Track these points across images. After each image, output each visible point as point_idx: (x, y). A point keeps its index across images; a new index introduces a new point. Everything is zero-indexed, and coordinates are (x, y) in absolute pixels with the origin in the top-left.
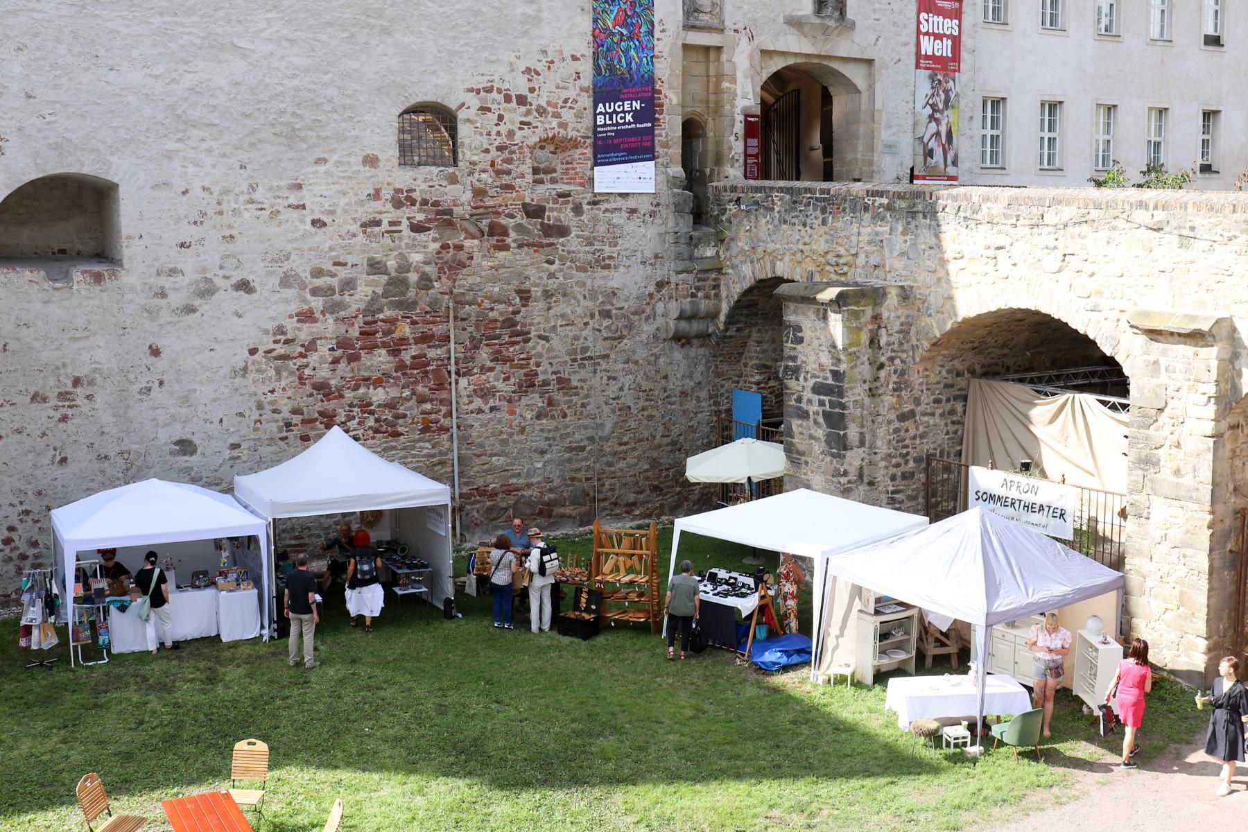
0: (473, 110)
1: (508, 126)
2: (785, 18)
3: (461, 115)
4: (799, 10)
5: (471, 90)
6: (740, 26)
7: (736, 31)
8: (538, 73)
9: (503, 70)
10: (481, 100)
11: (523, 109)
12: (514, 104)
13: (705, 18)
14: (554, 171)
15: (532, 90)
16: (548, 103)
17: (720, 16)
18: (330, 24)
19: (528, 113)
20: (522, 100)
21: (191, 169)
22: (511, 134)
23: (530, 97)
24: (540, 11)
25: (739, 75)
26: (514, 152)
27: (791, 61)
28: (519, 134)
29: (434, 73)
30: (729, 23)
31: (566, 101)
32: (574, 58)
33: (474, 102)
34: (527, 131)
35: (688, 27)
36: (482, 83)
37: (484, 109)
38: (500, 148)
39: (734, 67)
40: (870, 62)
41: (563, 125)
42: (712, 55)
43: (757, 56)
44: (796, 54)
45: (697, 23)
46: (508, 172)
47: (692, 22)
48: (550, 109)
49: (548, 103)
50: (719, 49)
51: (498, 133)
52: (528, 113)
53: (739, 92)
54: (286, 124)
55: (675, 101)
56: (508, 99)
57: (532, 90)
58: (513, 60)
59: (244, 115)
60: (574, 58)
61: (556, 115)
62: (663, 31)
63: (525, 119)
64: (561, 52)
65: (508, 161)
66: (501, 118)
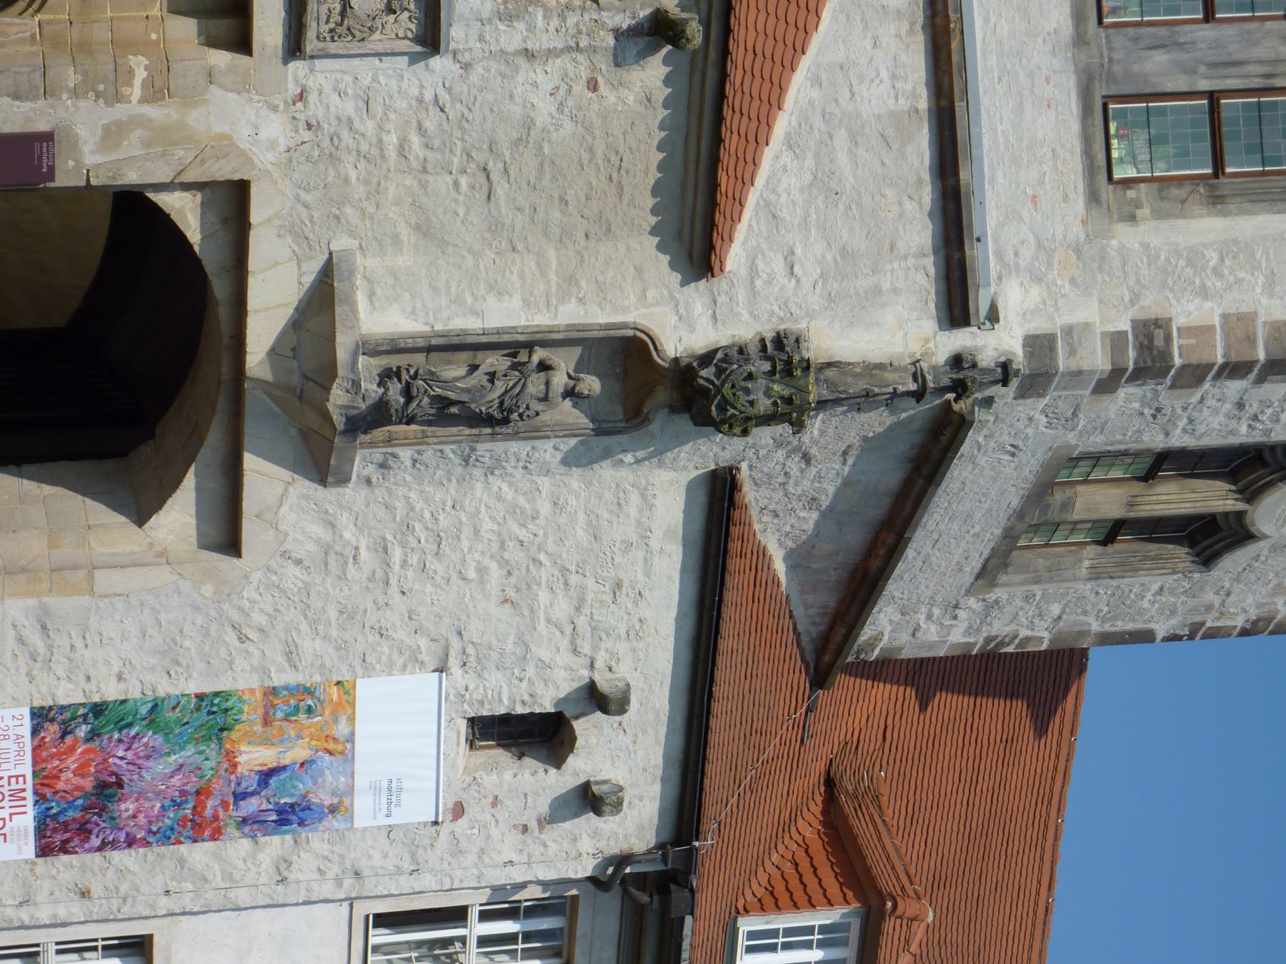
2: (347, 253)
4: (371, 295)
6: (315, 109)
7: (301, 97)
27: (220, 288)
42: (223, 26)
53: (120, 112)
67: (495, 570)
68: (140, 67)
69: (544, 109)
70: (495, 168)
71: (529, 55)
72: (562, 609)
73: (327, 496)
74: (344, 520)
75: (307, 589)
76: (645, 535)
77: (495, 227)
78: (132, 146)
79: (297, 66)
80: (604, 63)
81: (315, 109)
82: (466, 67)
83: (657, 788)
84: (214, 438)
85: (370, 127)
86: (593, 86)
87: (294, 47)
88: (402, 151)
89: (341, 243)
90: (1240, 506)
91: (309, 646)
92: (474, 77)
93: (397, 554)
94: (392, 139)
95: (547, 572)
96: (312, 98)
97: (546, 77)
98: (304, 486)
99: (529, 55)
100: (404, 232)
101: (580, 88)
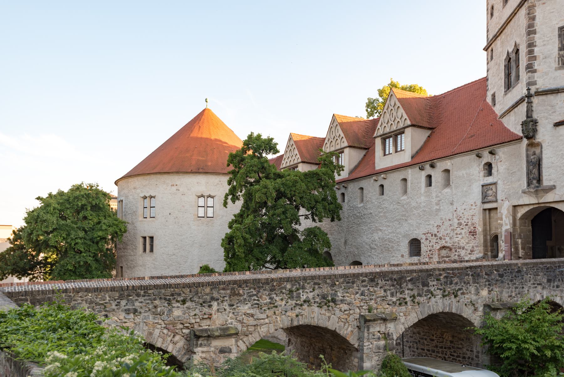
0: (424, 240)
1: (432, 244)
3: (422, 241)
5: (423, 234)
6: (504, 198)
7: (502, 200)
8: (440, 226)
9: (431, 227)
10: (426, 237)
11: (436, 238)
12: (434, 237)
13: (490, 198)
14: (450, 257)
15: (438, 232)
16: (442, 235)
17: (496, 197)
18: (395, 220)
19: (437, 239)
21: (372, 259)
22: (433, 246)
23: (438, 234)
24: (440, 207)
25: (504, 217)
26: (433, 252)
28: (435, 246)
29: (416, 230)
30: (499, 198)
31: (447, 234)
32: (450, 220)
33: (424, 237)
35: (483, 203)
36: (426, 231)
37: (427, 239)
38: (430, 251)
39: (502, 214)
41: (446, 242)
43: (511, 209)
44: (533, 204)
45: (487, 201)
46: (432, 258)
47: (486, 200)
48: (443, 237)
49: (442, 235)
50: (496, 209)
51: (430, 246)
52: (437, 239)
53: (504, 224)
54: (387, 247)
55: (480, 230)
57: (438, 232)
58: (434, 223)
59: (380, 246)
60: (450, 220)
61: (445, 239)
62: (476, 206)
63: (436, 241)
64: (446, 219)
65: (432, 254)
66: (430, 241)
68: (499, 221)
70: (511, 172)
71: (498, 171)
81: (504, 198)
82: (499, 179)
85: (506, 190)
86: (501, 161)
87: (496, 201)
88: (509, 185)
89: (521, 192)
92: (500, 177)
94: (507, 187)
96: (502, 199)
99: (498, 171)
100: (519, 183)
101: (501, 163)
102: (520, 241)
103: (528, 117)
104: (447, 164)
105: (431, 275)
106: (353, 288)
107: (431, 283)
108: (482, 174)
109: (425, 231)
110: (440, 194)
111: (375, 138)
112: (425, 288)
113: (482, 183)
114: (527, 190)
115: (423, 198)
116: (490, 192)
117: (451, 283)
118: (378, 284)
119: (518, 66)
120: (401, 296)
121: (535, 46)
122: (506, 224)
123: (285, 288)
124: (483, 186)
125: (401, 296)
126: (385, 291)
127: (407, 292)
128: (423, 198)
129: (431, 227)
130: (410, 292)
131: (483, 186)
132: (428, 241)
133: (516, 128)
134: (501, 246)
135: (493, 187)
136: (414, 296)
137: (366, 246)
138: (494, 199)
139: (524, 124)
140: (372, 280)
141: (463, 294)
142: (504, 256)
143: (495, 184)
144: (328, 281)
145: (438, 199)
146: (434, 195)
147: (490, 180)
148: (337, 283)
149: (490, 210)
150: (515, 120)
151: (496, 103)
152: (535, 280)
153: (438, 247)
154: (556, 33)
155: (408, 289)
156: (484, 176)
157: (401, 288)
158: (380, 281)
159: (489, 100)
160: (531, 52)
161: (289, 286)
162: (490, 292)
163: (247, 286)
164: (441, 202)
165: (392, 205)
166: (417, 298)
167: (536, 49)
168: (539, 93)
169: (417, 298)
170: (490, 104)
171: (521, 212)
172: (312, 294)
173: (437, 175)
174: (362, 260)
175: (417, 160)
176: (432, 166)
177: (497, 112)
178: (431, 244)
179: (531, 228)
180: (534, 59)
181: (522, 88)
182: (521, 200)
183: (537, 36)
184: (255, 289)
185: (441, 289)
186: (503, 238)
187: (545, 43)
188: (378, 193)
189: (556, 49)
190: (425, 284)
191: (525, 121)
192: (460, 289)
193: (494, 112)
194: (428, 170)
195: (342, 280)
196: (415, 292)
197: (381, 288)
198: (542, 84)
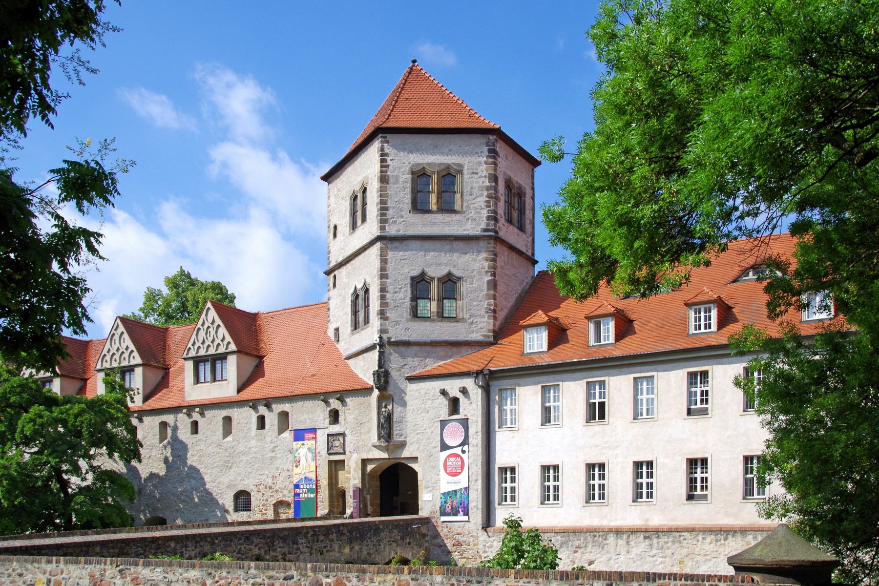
19: (272, 492)
20: (270, 488)
22: (267, 500)
25: (352, 470)
27: (381, 462)
28: (269, 500)
30: (348, 449)
32: (288, 470)
34: (272, 498)
35: (330, 454)
38: (263, 505)
39: (350, 468)
40: (417, 458)
41: (284, 496)
50: (343, 461)
52: (272, 492)
53: (352, 478)
56: (266, 487)
67: (423, 414)
69: (353, 416)
72: (430, 402)
73: (408, 443)
74: (412, 441)
75: (424, 446)
76: (417, 390)
77: (368, 421)
78: (356, 476)
79: (347, 453)
80: (346, 408)
81: (352, 450)
83: (464, 380)
84: (403, 461)
87: (344, 453)
89: (370, 445)
90: (436, 280)
91: (434, 444)
93: (419, 431)
95: (423, 406)
97: (348, 416)
98: (407, 447)
102: (368, 497)
103: (380, 366)
104: (286, 407)
105: (300, 533)
106: (230, 546)
107: (300, 541)
108: (327, 421)
109: (256, 481)
110: (276, 440)
111: (185, 359)
112: (295, 546)
113: (327, 431)
114: (378, 444)
115: (253, 442)
116: (337, 443)
117: (318, 541)
118: (253, 542)
119: (367, 307)
120: (274, 554)
121: (387, 292)
122: (355, 479)
123: (169, 546)
124: (328, 435)
125: (274, 554)
126: (259, 549)
127: (279, 550)
128: (253, 442)
129: (265, 477)
130: (281, 549)
131: (328, 435)
132: (261, 494)
133: (365, 375)
134: (348, 502)
135: (341, 438)
136: (285, 554)
137: (172, 498)
138: (342, 451)
139: (377, 375)
140: (248, 538)
141: (328, 551)
142: (352, 513)
143: (343, 435)
144: (209, 539)
145: (274, 445)
146: (268, 439)
147: (335, 429)
148: (217, 541)
149: (336, 462)
150: (364, 366)
151: (340, 339)
152: (390, 538)
153: (274, 502)
154: (408, 281)
155: (280, 547)
156: (330, 424)
157: (273, 545)
158: (255, 539)
159: (331, 333)
160: (383, 297)
161: (173, 545)
162: (352, 549)
163: (134, 545)
164: (277, 449)
165: (210, 447)
166: (288, 555)
167: (388, 295)
168: (390, 343)
169: (288, 555)
170: (333, 338)
171: (370, 468)
172: (194, 552)
173: (272, 419)
174: (166, 515)
175: (247, 394)
176: (268, 406)
177: (341, 351)
178: (265, 498)
179: (379, 482)
180: (385, 305)
181: (373, 333)
182: (371, 453)
183: (389, 281)
184: (142, 547)
185: (308, 547)
186: (351, 493)
187: (397, 290)
188: (190, 431)
189: (408, 299)
190: (295, 542)
191: (377, 371)
192: (325, 547)
193: (337, 350)
194: (262, 410)
195: (220, 538)
196: (286, 550)
197: (256, 546)
198: (396, 334)
